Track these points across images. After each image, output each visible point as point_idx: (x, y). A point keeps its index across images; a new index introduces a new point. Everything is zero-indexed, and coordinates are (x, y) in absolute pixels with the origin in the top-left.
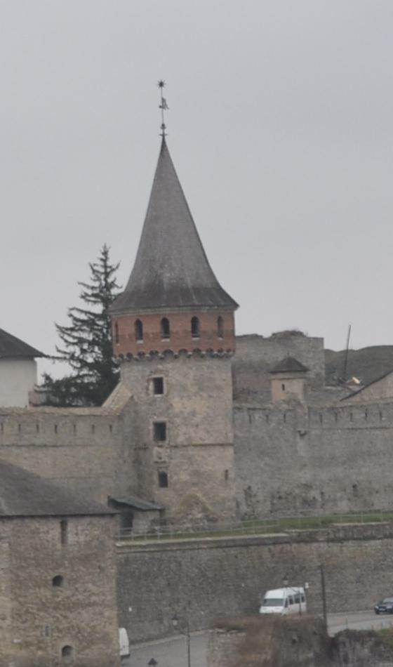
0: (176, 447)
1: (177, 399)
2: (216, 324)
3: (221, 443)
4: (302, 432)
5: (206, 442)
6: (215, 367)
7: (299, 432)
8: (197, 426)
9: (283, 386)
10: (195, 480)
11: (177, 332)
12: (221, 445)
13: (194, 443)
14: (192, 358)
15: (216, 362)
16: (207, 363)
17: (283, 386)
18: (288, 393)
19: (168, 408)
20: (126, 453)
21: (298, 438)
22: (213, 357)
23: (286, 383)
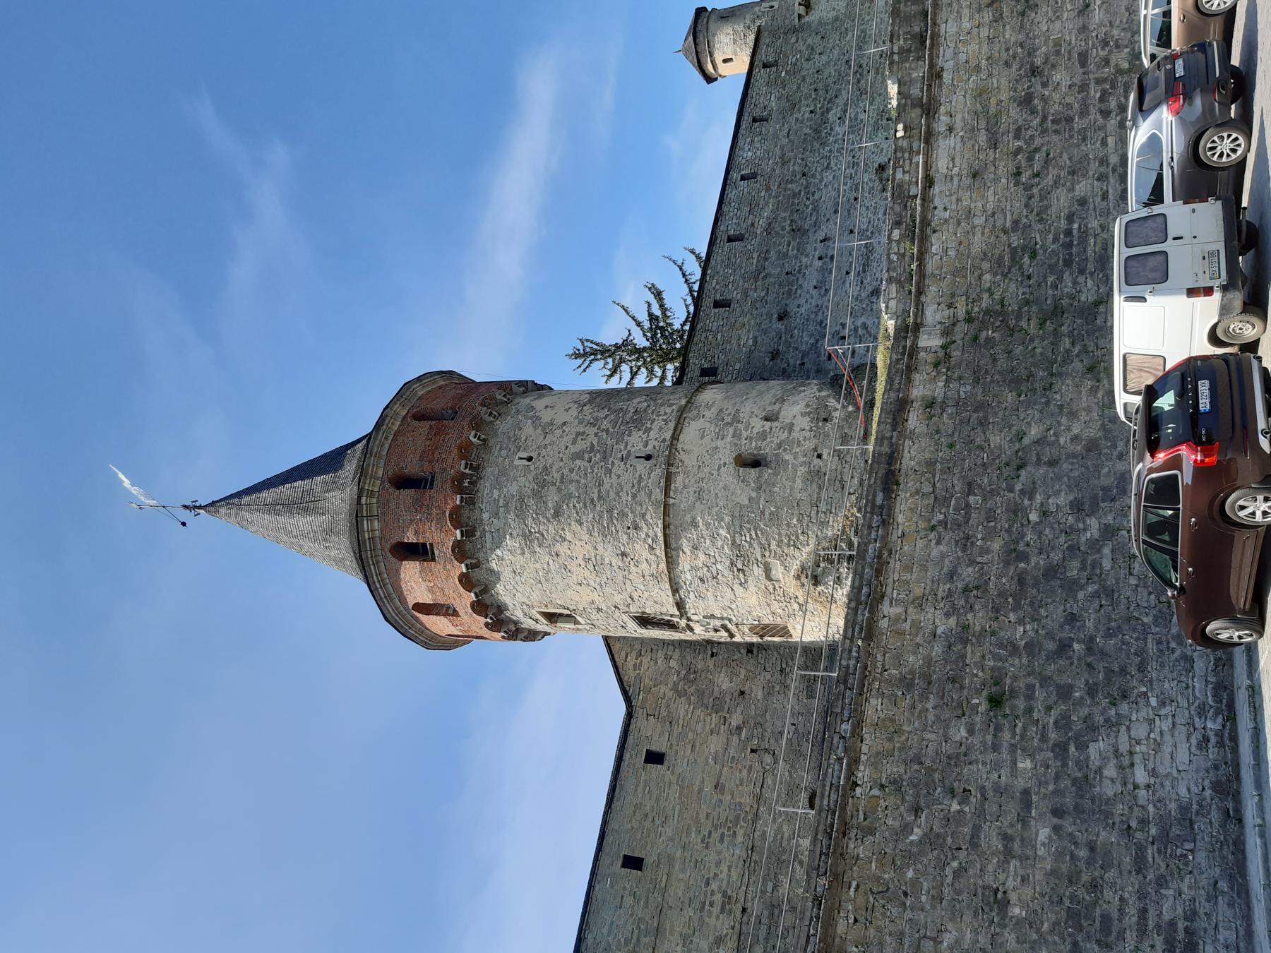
0: (680, 605)
1: (570, 593)
2: (404, 492)
3: (663, 483)
4: (802, 10)
5: (660, 534)
6: (496, 493)
7: (800, 16)
8: (624, 554)
9: (725, 61)
10: (758, 571)
11: (431, 590)
12: (669, 477)
13: (663, 566)
14: (480, 555)
15: (486, 489)
16: (486, 516)
17: (725, 61)
18: (735, 53)
19: (599, 610)
20: (724, 682)
21: (812, 18)
22: (471, 502)
23: (719, 58)
